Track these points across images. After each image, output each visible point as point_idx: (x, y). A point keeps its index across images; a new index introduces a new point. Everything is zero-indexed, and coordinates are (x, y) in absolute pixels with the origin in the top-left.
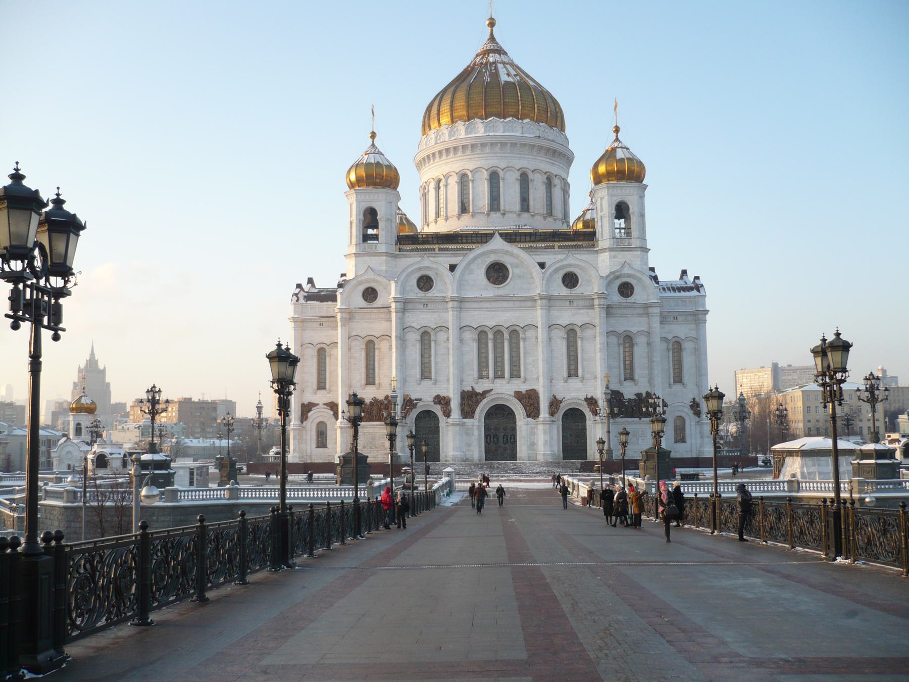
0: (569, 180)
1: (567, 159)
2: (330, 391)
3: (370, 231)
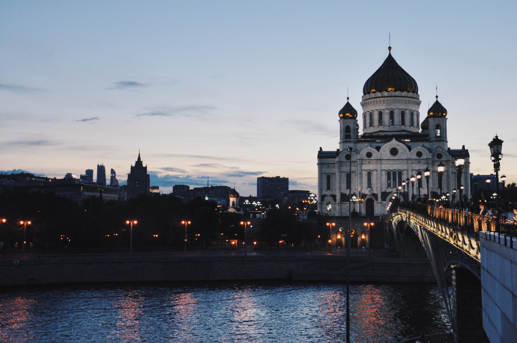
0: (420, 111)
1: (419, 104)
2: (332, 190)
3: (347, 134)
